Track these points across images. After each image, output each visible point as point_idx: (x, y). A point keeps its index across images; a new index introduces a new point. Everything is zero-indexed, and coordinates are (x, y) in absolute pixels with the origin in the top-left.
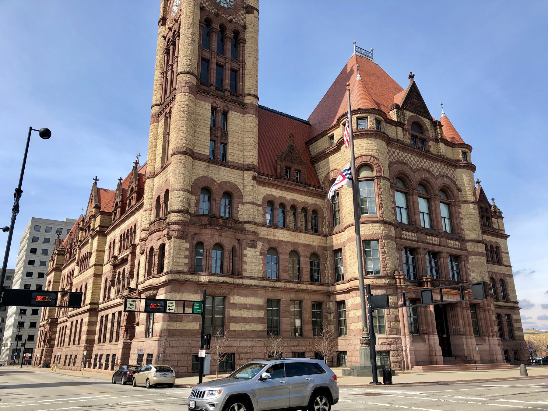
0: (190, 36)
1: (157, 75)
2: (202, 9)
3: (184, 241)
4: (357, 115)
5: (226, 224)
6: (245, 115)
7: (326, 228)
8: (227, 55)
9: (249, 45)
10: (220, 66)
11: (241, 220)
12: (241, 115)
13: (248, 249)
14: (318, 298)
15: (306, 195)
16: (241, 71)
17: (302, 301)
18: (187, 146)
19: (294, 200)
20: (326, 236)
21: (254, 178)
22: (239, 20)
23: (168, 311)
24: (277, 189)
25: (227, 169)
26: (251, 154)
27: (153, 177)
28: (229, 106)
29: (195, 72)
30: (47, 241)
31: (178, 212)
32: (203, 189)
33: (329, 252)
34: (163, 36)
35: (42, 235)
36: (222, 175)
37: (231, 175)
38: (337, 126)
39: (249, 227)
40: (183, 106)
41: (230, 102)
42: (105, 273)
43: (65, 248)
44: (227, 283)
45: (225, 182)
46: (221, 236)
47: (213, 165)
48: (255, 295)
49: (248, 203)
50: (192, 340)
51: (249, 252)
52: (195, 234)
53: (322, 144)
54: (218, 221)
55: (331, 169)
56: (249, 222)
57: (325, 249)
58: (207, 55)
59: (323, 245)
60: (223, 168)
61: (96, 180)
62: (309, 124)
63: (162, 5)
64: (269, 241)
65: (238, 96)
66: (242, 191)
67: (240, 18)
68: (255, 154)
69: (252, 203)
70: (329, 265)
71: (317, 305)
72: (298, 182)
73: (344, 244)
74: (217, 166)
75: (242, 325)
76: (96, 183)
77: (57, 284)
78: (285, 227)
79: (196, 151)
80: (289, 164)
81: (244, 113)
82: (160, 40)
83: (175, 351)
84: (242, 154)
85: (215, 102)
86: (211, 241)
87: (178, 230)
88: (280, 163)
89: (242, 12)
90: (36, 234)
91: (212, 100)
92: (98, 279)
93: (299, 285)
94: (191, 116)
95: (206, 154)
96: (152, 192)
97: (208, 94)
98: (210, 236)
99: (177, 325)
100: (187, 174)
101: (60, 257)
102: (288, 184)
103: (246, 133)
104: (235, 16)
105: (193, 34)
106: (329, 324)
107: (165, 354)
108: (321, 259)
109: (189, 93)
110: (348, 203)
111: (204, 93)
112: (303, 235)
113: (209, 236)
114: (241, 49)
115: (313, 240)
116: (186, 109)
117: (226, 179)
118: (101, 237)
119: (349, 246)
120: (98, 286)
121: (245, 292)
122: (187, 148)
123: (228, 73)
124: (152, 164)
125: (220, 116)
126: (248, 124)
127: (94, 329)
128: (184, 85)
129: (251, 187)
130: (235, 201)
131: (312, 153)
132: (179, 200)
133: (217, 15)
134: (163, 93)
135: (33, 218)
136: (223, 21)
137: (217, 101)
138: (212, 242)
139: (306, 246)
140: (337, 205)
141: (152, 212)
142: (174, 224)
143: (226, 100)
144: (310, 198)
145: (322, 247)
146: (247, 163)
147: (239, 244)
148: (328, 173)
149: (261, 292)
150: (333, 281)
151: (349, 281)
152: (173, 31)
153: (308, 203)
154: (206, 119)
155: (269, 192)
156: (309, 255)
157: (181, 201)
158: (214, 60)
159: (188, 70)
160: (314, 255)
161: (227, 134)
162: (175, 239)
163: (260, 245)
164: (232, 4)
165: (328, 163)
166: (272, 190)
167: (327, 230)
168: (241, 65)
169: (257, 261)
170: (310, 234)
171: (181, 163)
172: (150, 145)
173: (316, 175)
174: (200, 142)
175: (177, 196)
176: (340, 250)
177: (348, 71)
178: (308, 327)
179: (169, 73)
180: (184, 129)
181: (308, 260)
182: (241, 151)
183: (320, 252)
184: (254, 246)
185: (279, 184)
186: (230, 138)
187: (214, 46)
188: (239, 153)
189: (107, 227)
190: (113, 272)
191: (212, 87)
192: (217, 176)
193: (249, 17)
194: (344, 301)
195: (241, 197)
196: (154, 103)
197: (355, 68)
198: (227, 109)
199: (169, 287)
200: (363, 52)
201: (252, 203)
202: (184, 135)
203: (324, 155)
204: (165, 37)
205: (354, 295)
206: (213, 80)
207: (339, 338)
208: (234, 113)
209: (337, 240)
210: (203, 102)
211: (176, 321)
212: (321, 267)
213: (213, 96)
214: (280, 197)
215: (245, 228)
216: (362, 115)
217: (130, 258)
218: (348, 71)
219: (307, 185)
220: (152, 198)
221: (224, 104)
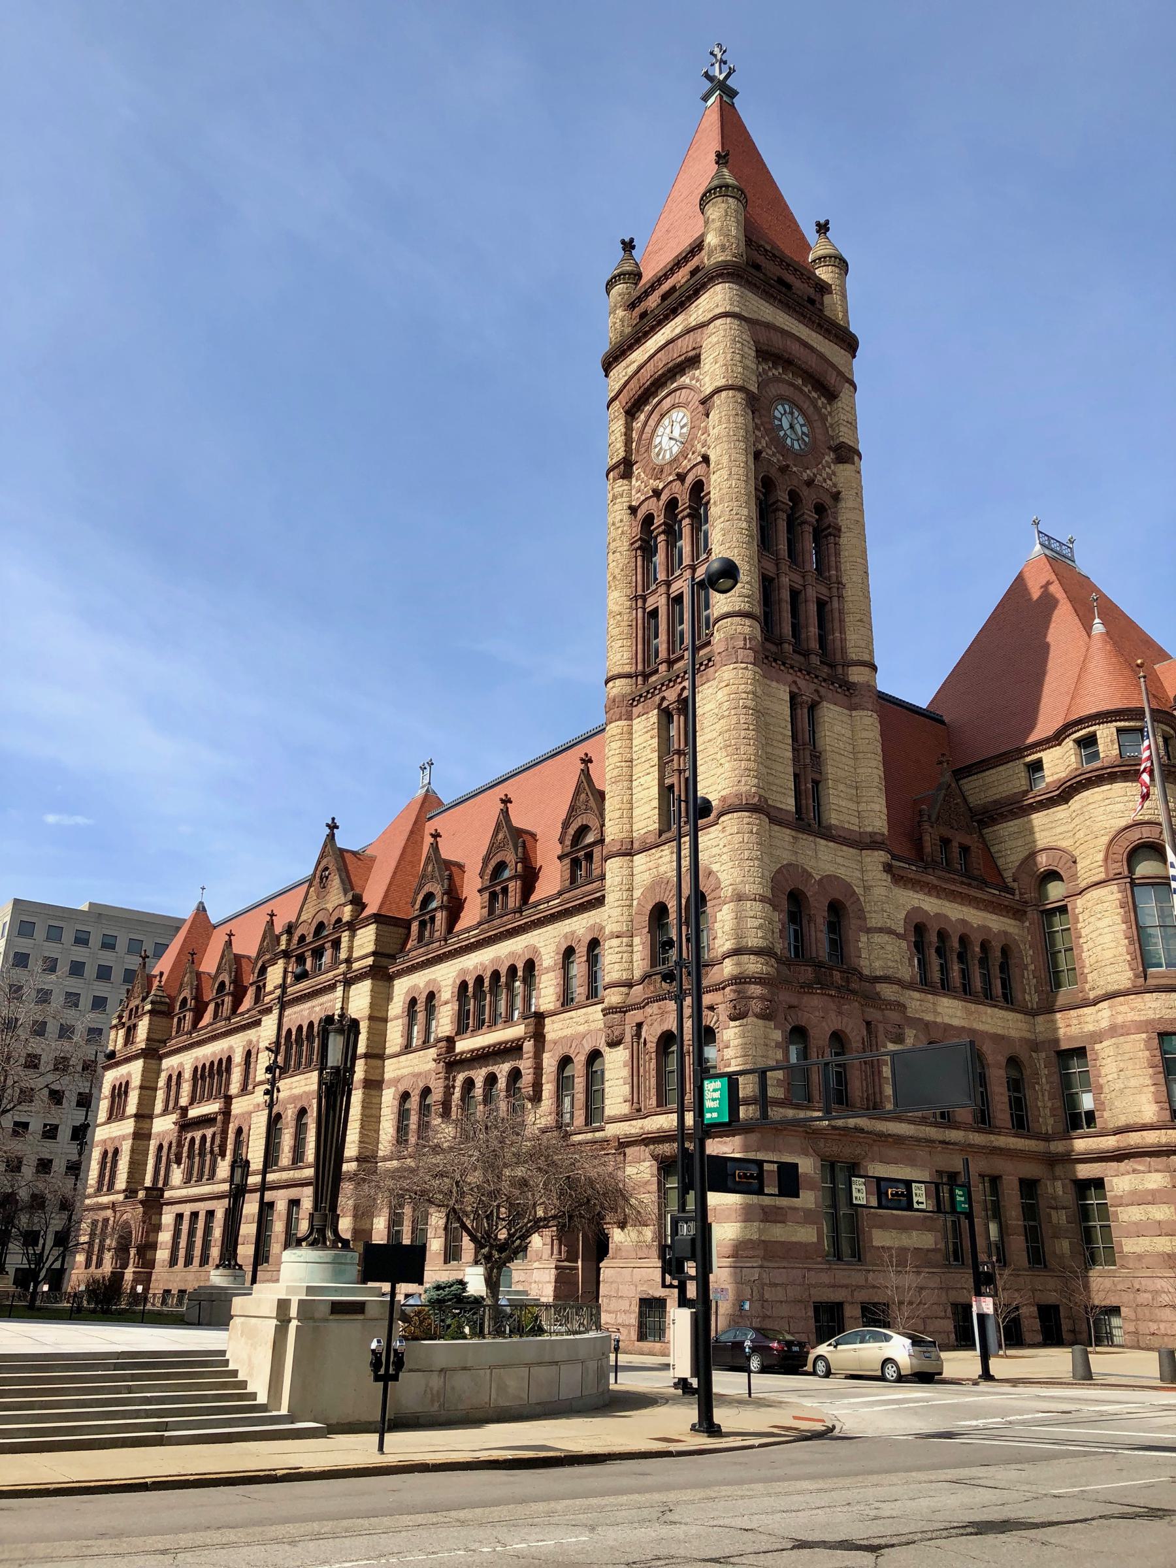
0: (744, 525)
1: (617, 599)
2: (757, 455)
3: (772, 1024)
4: (1119, 724)
5: (848, 982)
6: (854, 713)
7: (1030, 994)
8: (807, 568)
9: (846, 539)
10: (795, 594)
11: (866, 972)
12: (846, 711)
14: (1031, 1170)
15: (986, 909)
16: (835, 605)
17: (1000, 1177)
18: (761, 792)
19: (963, 922)
20: (1033, 1013)
21: (888, 868)
22: (825, 480)
23: (916, 1206)
24: (929, 894)
25: (831, 844)
26: (877, 807)
27: (628, 852)
28: (823, 691)
29: (757, 610)
30: (104, 973)
31: (758, 952)
32: (790, 898)
33: (1043, 1055)
34: (630, 507)
35: (39, 947)
36: (826, 861)
37: (839, 860)
38: (1056, 739)
39: (887, 991)
40: (744, 696)
41: (825, 680)
42: (398, 1080)
43: (173, 999)
44: (862, 1130)
45: (831, 879)
46: (840, 1013)
47: (805, 836)
48: (912, 1162)
49: (880, 930)
50: (809, 1269)
52: (790, 1007)
53: (1007, 780)
54: (831, 975)
55: (1041, 844)
56: (886, 979)
57: (1034, 1046)
58: (771, 570)
59: (1028, 1035)
60: (823, 842)
61: (333, 826)
62: (942, 722)
63: (618, 426)
64: (927, 1026)
65: (832, 666)
66: (862, 899)
67: (825, 475)
68: (832, 799)
69: (890, 932)
70: (1047, 1087)
71: (1029, 1187)
72: (969, 876)
73: (1097, 1037)
74: (811, 838)
75: (894, 1233)
76: (331, 837)
77: (149, 1092)
78: (945, 987)
79: (770, 802)
80: (946, 832)
81: (852, 708)
82: (618, 513)
83: (780, 1294)
85: (795, 682)
86: (824, 1024)
87: (762, 998)
88: (930, 830)
89: (827, 458)
90: (24, 945)
91: (790, 678)
92: (373, 1092)
93: (992, 1137)
94: (760, 715)
95: (788, 808)
96: (631, 890)
97: (784, 664)
98: (822, 1014)
99: (778, 1233)
100: (766, 859)
101: (161, 1021)
102: (954, 881)
103: (860, 755)
104: (815, 470)
105: (749, 520)
106: (1056, 1236)
107: (762, 1300)
108: (1027, 1072)
109: (754, 664)
110: (1108, 938)
111: (775, 660)
112: (989, 1010)
113: (823, 1015)
114: (832, 551)
115: (994, 1021)
116: (750, 703)
117: (830, 869)
118: (380, 983)
119: (1117, 1046)
120: (374, 1112)
121: (893, 1153)
122: (760, 796)
123: (813, 608)
124: (625, 820)
125: (803, 713)
126: (865, 734)
127: (368, 1226)
128: (741, 644)
129: (883, 891)
130: (854, 923)
131: (970, 799)
132: (757, 923)
133: (784, 469)
134: (640, 647)
135: (17, 902)
136: (795, 482)
138: (827, 1028)
139: (997, 1038)
140: (1058, 936)
141: (637, 940)
142: (750, 983)
143: (817, 677)
144: (994, 917)
145: (1027, 1041)
146: (869, 829)
147: (869, 1032)
148: (1033, 855)
149: (922, 1154)
150: (1061, 1127)
151: (1118, 1131)
152: (664, 497)
153: (990, 929)
154: (783, 725)
155: (916, 903)
156: (1004, 1061)
157: (760, 927)
158: (785, 580)
159: (746, 607)
160: (1013, 1062)
161: (819, 757)
162: (755, 1019)
164: (807, 439)
165: (1031, 832)
166: (921, 896)
167: (1036, 998)
168: (835, 590)
170: (1001, 1008)
171: (751, 832)
172: (615, 772)
173: (991, 860)
174: (777, 781)
175: (752, 914)
176: (1081, 1052)
177: (1036, 594)
178: (1018, 1245)
179: (658, 600)
180: (751, 750)
181: (1002, 1073)
182: (851, 800)
183: (1023, 1055)
185: (935, 882)
186: (831, 770)
187: (783, 547)
189: (393, 957)
190: (447, 1078)
191: (786, 646)
192: (813, 863)
193: (843, 471)
194: (1102, 1179)
195: (861, 915)
196: (616, 671)
197: (1056, 589)
198: (817, 699)
199: (754, 1137)
200: (1055, 545)
201: (890, 932)
202: (753, 765)
203: (1019, 808)
204: (633, 510)
205: (1141, 1168)
206: (787, 630)
207: (1091, 1273)
208: (832, 707)
209: (1071, 1026)
210: (774, 684)
211: (775, 1222)
212: (1029, 1093)
213: (792, 667)
214: (937, 914)
215: (878, 994)
216: (1132, 724)
217: (528, 1046)
218: (1036, 594)
219: (983, 883)
220: (631, 906)
221: (813, 686)
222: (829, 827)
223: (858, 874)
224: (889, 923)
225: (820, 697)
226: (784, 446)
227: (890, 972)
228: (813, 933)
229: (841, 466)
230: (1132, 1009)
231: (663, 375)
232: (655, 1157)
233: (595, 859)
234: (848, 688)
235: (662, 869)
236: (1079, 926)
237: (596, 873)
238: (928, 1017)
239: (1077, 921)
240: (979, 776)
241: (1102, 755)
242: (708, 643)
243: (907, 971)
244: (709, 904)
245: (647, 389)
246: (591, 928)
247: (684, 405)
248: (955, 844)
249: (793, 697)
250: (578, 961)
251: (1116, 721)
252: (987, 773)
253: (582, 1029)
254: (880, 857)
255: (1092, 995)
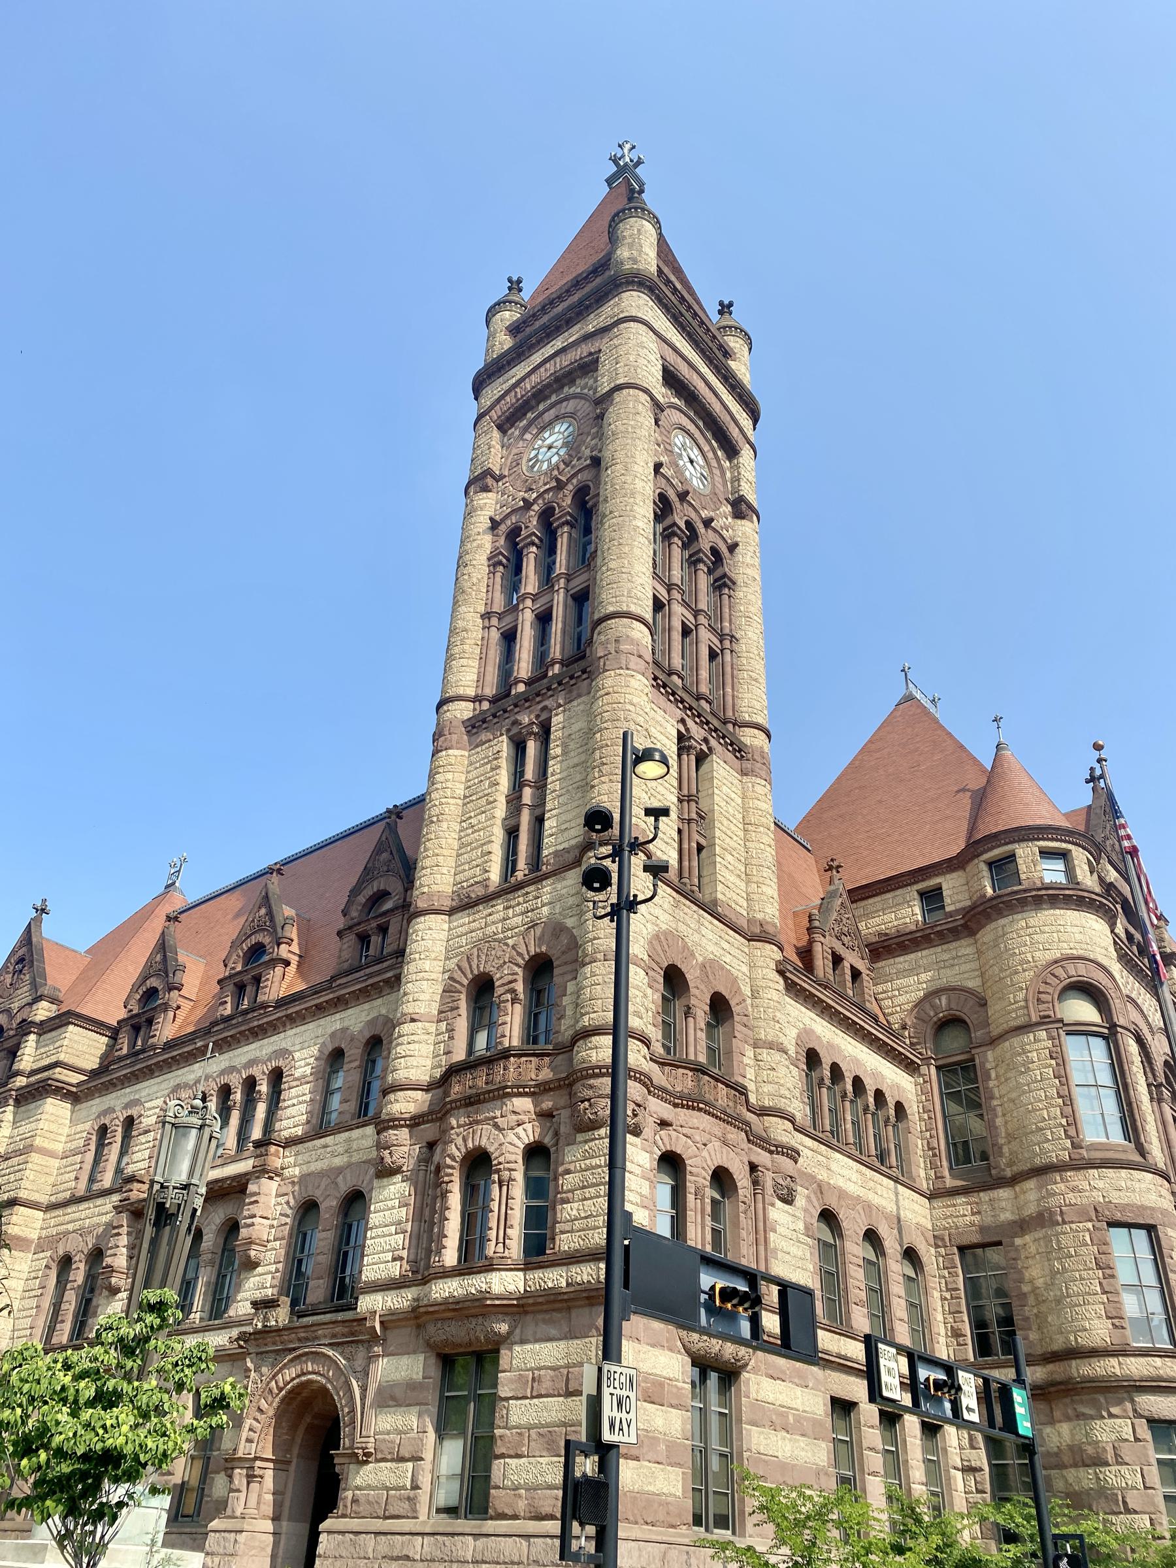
2: (658, 467)
13: (779, 1204)
19: (856, 1061)
28: (713, 743)
37: (726, 946)
51: (778, 1213)
66: (749, 1001)
84: (743, 885)
86: (705, 1153)
91: (679, 714)
129: (775, 996)
137: (690, 723)
146: (759, 916)
163: (802, 1196)
169: (800, 1253)
184: (788, 1200)
188: (738, 882)
222: (715, 902)
223: (745, 969)
224: (782, 1039)
225: (710, 749)
226: (682, 474)
227: (782, 1104)
228: (691, 1031)
229: (739, 522)
230: (1073, 1190)
231: (549, 385)
232: (430, 1346)
233: (390, 930)
234: (739, 751)
235: (491, 929)
236: (991, 1084)
237: (394, 947)
238: (822, 1175)
239: (989, 1078)
240: (866, 902)
241: (1023, 877)
242: (584, 657)
243: (799, 1109)
244: (556, 971)
245: (527, 402)
246: (372, 1023)
247: (572, 415)
248: (846, 964)
249: (681, 737)
250: (346, 1067)
251: (1039, 839)
252: (871, 901)
253: (338, 1161)
254: (769, 954)
255: (1008, 1173)
